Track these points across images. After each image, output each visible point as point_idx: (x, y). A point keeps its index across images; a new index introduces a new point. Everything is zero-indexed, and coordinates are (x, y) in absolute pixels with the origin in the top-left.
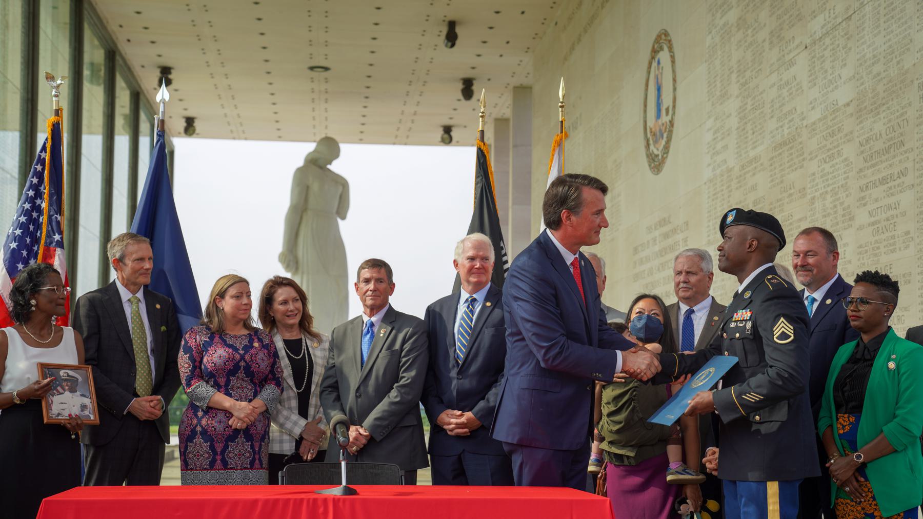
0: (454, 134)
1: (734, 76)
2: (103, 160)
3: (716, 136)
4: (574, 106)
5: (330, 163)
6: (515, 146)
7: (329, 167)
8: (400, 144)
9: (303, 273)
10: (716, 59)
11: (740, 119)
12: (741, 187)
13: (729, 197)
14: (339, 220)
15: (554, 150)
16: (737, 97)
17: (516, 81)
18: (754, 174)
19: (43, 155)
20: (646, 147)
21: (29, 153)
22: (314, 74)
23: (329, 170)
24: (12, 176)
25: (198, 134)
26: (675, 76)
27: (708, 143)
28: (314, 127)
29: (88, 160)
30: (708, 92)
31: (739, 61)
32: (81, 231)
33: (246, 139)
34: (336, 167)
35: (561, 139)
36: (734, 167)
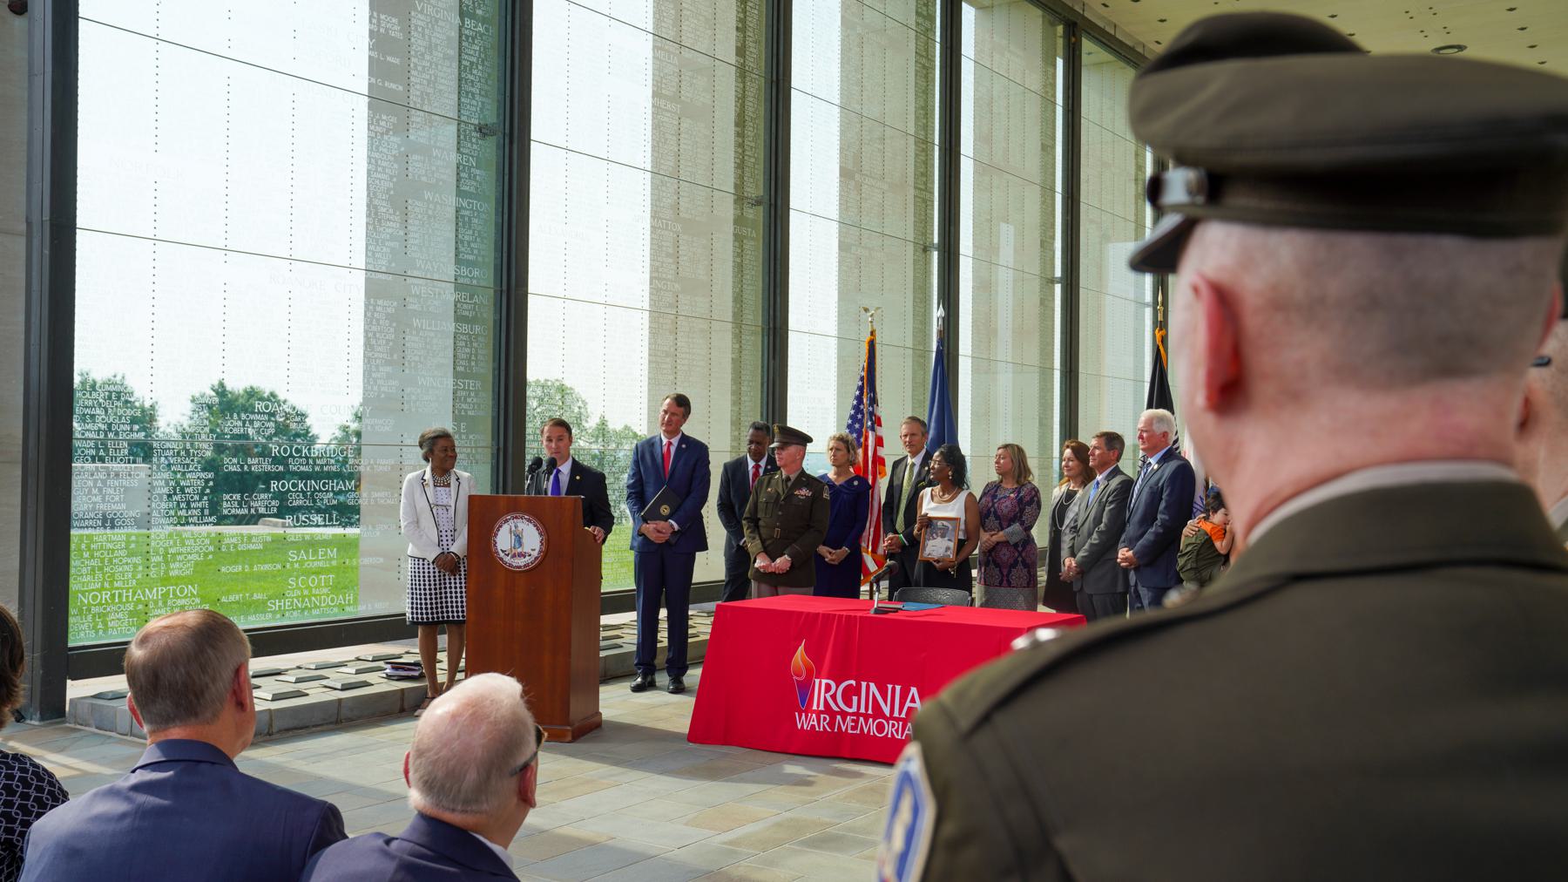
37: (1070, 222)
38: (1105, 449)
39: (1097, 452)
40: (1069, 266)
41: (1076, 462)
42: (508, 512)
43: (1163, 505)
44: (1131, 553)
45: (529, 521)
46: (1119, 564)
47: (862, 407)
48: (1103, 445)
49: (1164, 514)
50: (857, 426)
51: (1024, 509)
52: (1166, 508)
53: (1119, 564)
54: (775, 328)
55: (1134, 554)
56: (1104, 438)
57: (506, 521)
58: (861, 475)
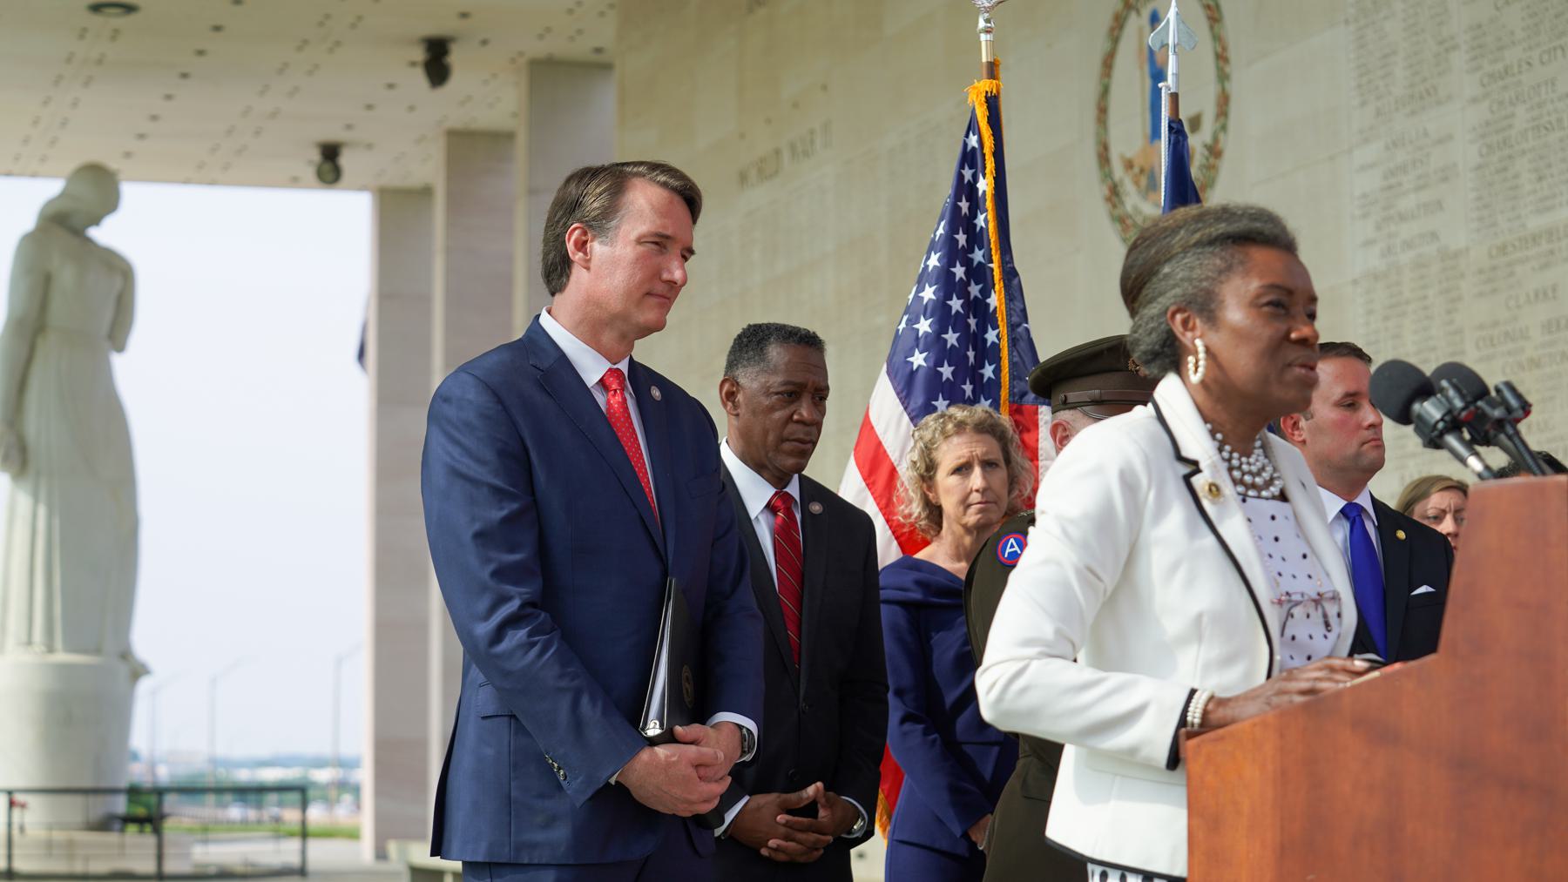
0: (345, 160)
1: (1459, 59)
3: (1393, 181)
4: (796, 105)
8: (200, 182)
10: (1386, 18)
11: (1489, 147)
12: (1494, 291)
13: (1449, 312)
16: (1474, 100)
17: (540, 49)
18: (1545, 266)
20: (1108, 199)
22: (97, 20)
23: (89, 241)
26: (1224, 49)
27: (1364, 196)
28: (26, 141)
30: (1359, 86)
31: (1479, 26)
34: (105, 234)
36: (1467, 249)
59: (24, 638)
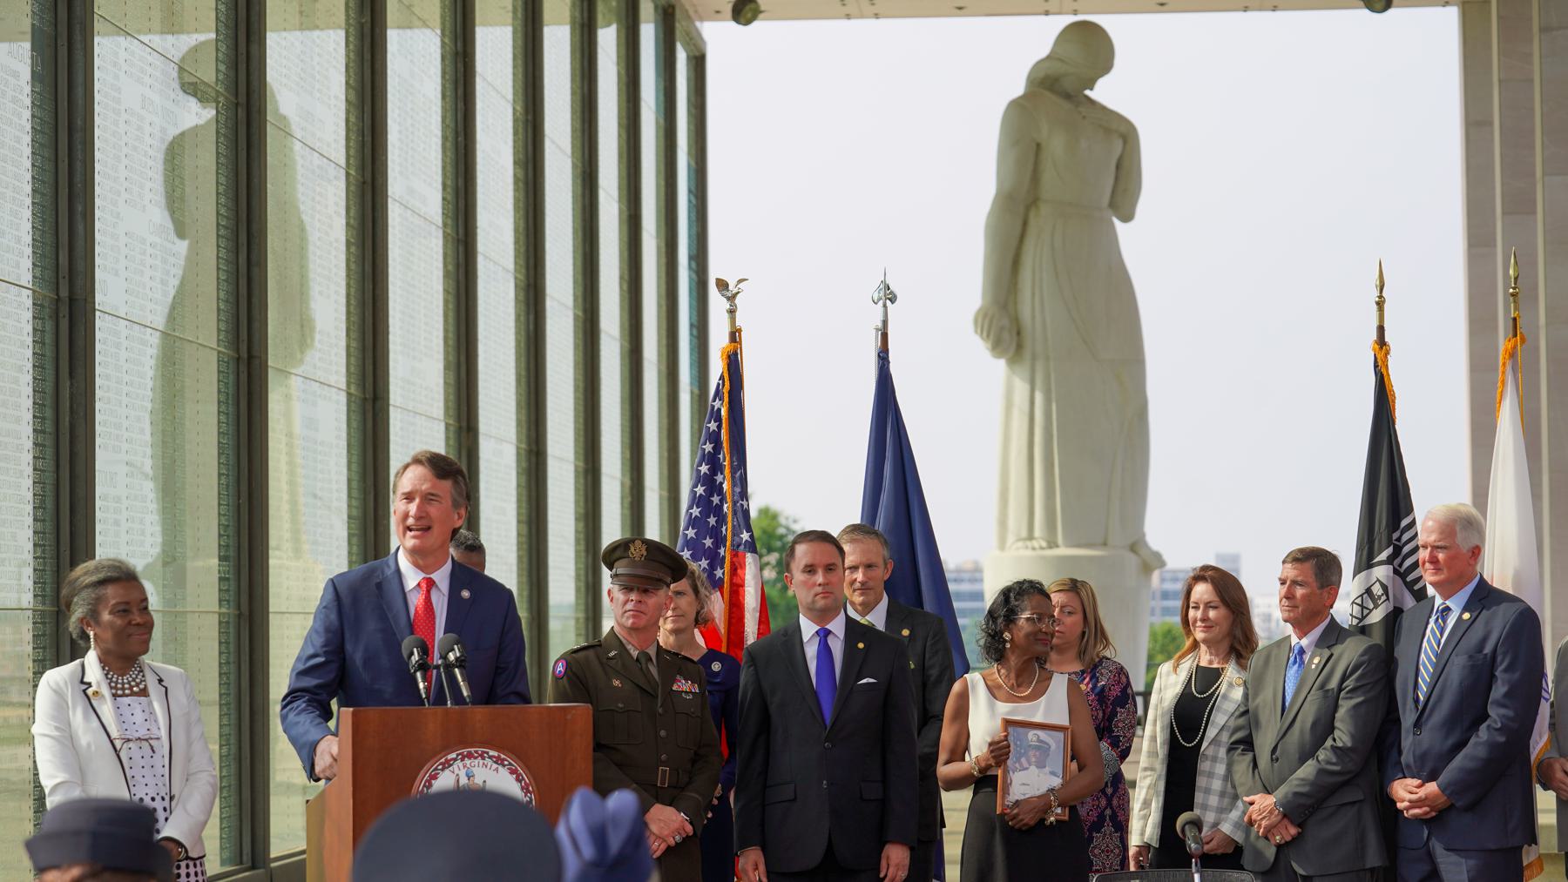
2: (573, 131)
5: (1091, 89)
6: (1543, 30)
7: (1087, 92)
8: (1260, 9)
9: (1034, 358)
14: (1117, 222)
15: (1504, 364)
19: (717, 404)
21: (462, 167)
24: (438, 227)
25: (761, 12)
29: (553, 142)
32: (550, 304)
33: (877, 16)
34: (1104, 92)
35: (1515, 347)
37: (368, 27)
38: (1315, 584)
39: (1299, 592)
40: (368, 139)
41: (1223, 611)
42: (448, 748)
43: (1499, 690)
44: (1432, 787)
45: (499, 761)
46: (1402, 812)
47: (716, 499)
48: (1311, 579)
49: (1504, 706)
50: (708, 542)
51: (1114, 714)
52: (1506, 695)
53: (1402, 812)
54: (72, 300)
55: (1443, 789)
56: (1309, 566)
57: (447, 765)
58: (724, 650)
59: (1024, 534)
